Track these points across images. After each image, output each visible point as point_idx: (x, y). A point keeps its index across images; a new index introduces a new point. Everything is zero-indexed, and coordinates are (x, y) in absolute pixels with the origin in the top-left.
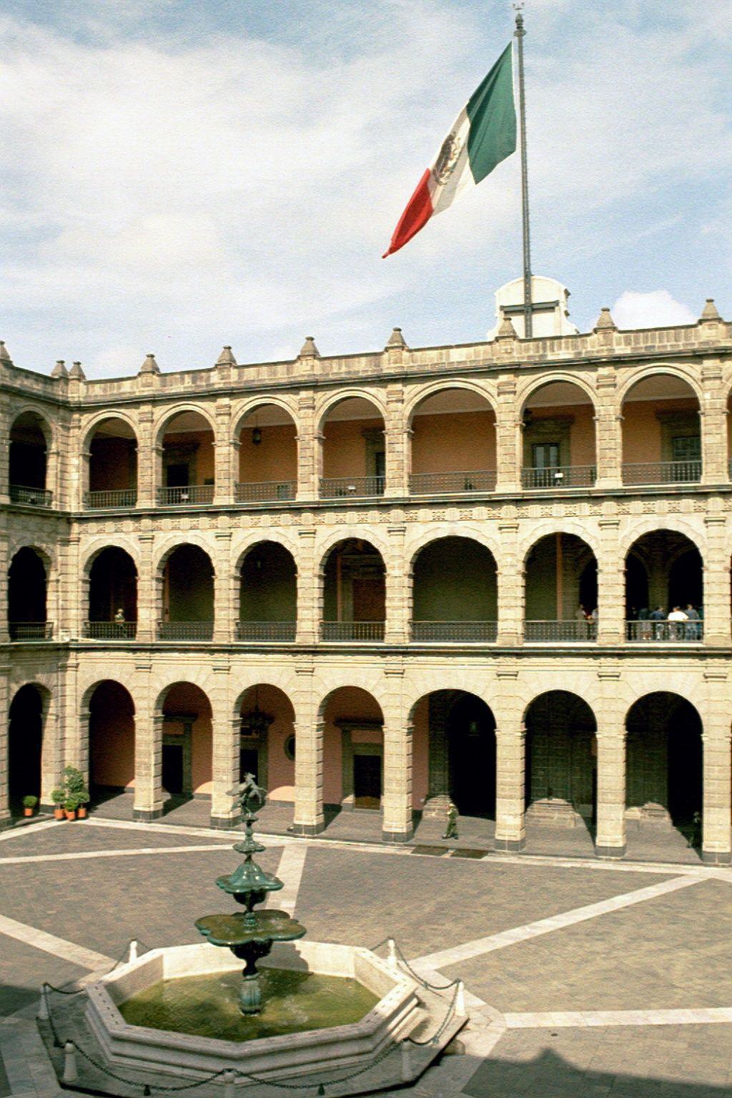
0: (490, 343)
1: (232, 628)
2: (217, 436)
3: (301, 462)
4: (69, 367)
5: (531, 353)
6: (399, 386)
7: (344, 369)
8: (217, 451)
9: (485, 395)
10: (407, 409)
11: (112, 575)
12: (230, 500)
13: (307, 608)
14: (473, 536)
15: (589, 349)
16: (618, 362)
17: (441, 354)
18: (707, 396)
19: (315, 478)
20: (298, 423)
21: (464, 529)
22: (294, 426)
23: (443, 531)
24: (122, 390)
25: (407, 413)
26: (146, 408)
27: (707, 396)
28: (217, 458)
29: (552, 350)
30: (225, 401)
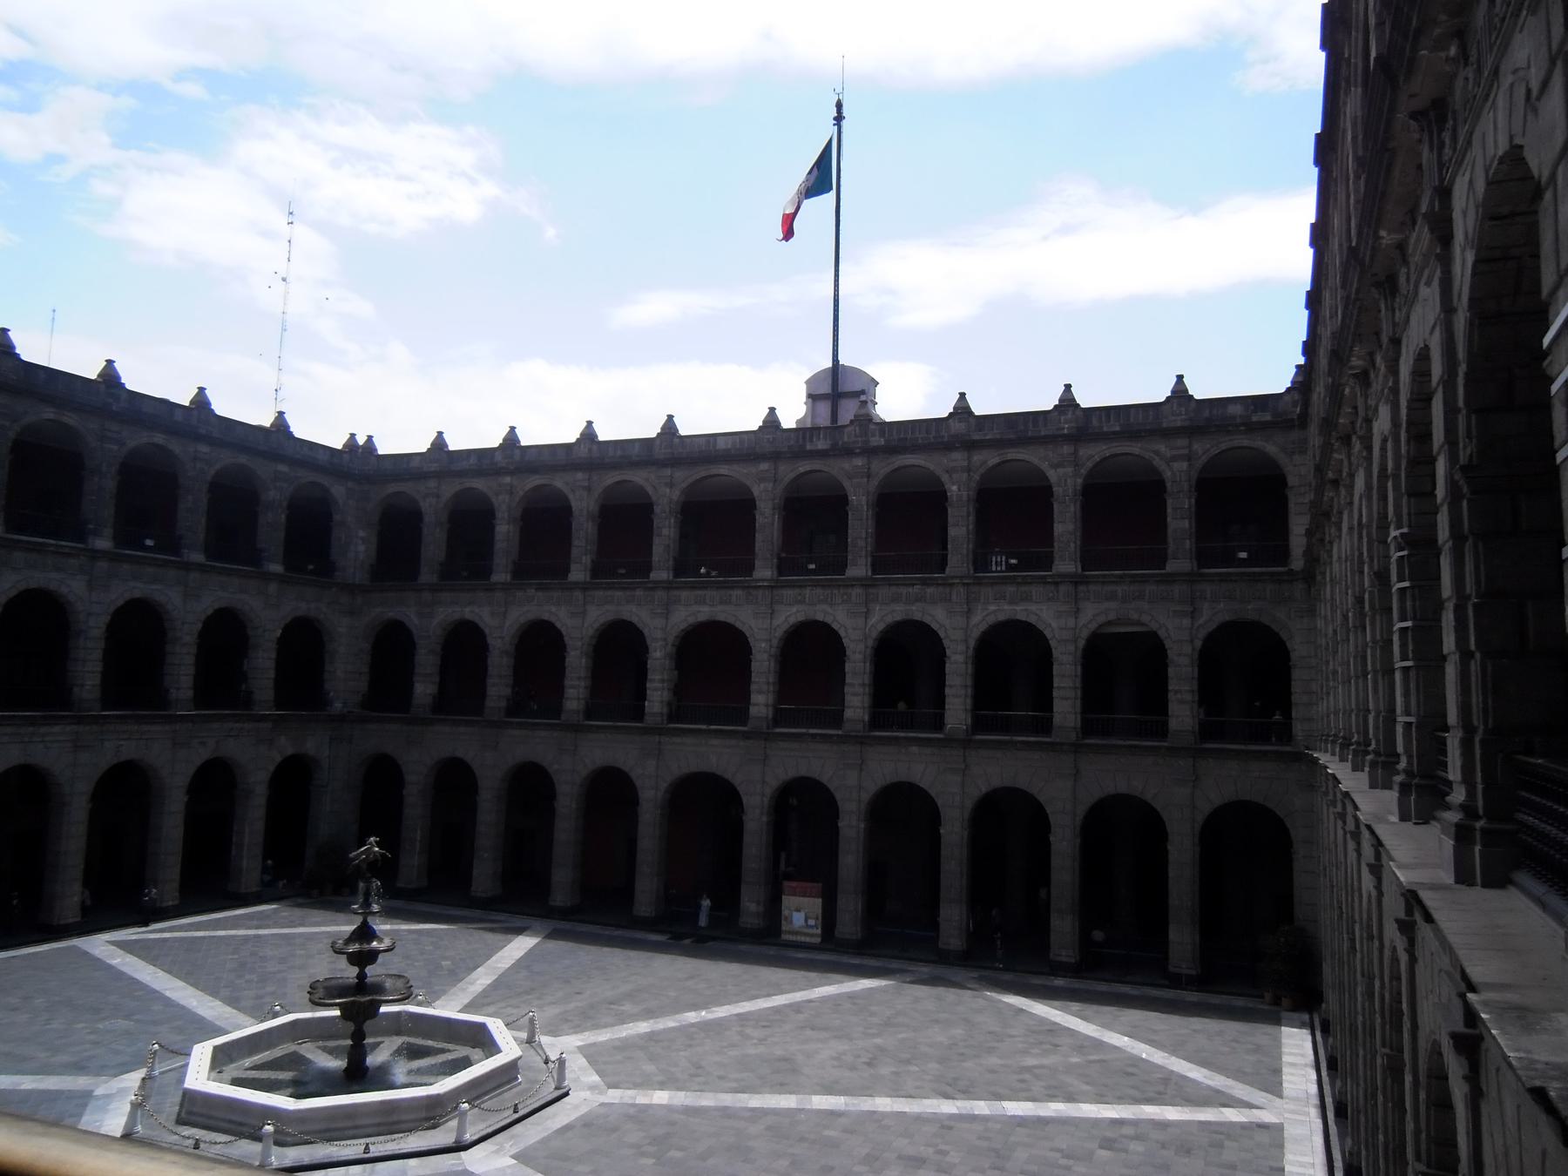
1: (503, 704)
2: (499, 515)
3: (576, 542)
4: (361, 440)
8: (498, 529)
10: (676, 494)
11: (392, 646)
13: (573, 687)
14: (731, 620)
16: (870, 452)
18: (955, 488)
19: (587, 560)
20: (574, 504)
21: (723, 613)
22: (570, 508)
23: (704, 613)
25: (675, 498)
26: (432, 484)
27: (955, 488)
28: (498, 537)
30: (508, 479)
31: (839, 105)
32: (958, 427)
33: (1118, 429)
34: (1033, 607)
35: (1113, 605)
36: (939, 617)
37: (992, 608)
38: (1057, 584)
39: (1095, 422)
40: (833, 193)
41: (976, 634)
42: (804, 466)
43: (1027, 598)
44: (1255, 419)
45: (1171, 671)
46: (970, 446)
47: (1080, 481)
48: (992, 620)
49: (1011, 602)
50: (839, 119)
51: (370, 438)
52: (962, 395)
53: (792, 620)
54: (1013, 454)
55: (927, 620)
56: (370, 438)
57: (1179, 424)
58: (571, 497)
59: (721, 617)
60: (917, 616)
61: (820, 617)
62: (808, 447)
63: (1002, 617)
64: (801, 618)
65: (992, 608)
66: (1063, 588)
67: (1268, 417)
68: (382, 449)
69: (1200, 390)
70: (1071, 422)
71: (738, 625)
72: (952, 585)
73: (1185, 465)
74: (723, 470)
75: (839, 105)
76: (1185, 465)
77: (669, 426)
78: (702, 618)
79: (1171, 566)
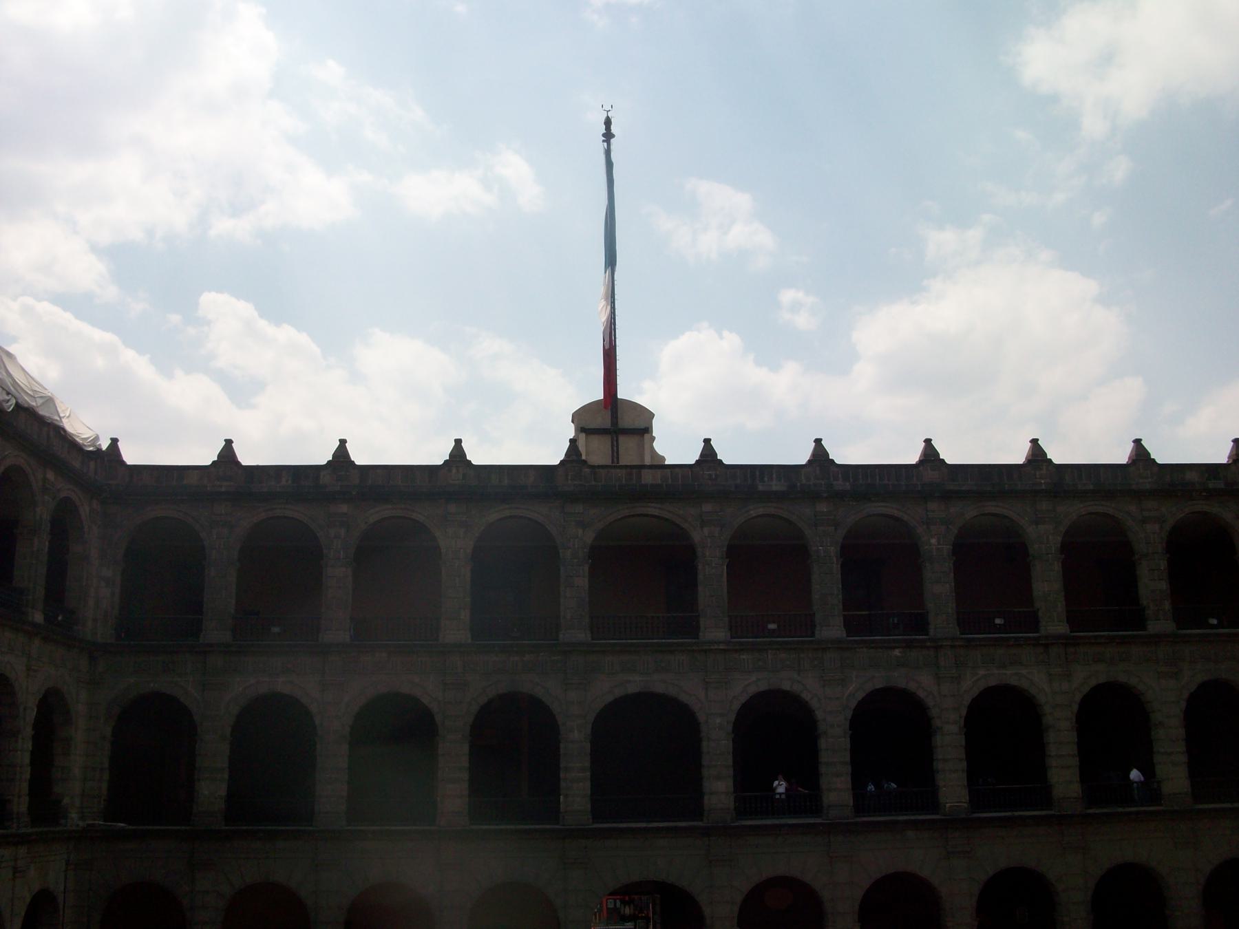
5: (738, 481)
7: (506, 482)
9: (685, 526)
10: (589, 537)
12: (582, 636)
15: (804, 482)
21: (661, 684)
23: (634, 683)
24: (185, 482)
30: (344, 508)
31: (608, 122)
32: (930, 475)
33: (1091, 487)
36: (923, 683)
37: (982, 672)
38: (1046, 646)
41: (967, 700)
42: (756, 510)
44: (1211, 486)
45: (822, 743)
46: (948, 496)
47: (1059, 539)
48: (982, 685)
50: (608, 136)
51: (114, 441)
53: (753, 690)
54: (992, 507)
55: (912, 686)
56: (114, 441)
57: (1148, 487)
59: (659, 688)
60: (901, 683)
61: (786, 686)
62: (760, 488)
63: (993, 682)
64: (763, 686)
65: (982, 672)
67: (1221, 485)
68: (131, 456)
71: (684, 698)
72: (941, 646)
73: (1157, 527)
74: (653, 509)
75: (608, 122)
76: (1157, 527)
78: (632, 689)
79: (1153, 627)
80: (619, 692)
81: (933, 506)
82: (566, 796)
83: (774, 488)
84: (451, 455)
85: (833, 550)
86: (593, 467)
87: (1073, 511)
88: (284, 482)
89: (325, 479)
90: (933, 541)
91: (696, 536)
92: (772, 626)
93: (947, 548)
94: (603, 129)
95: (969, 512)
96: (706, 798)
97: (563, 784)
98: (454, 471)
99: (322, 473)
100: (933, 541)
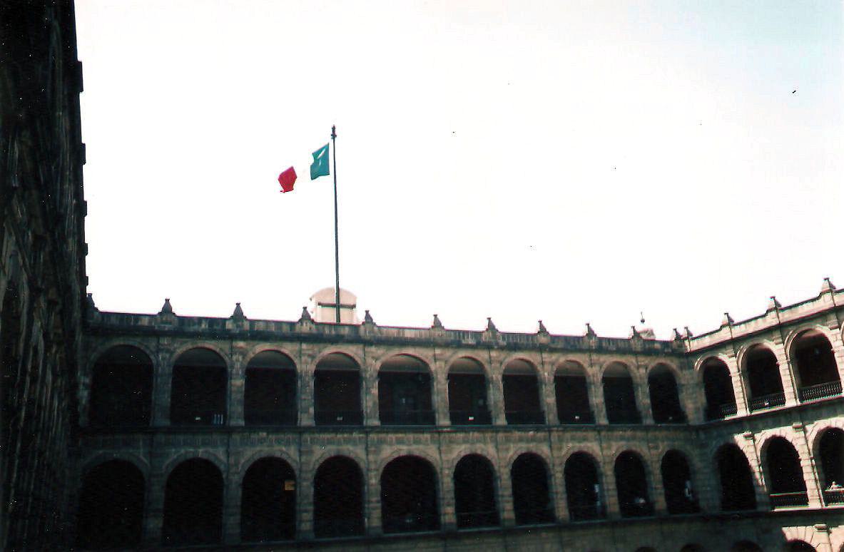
0: (429, 329)
6: (373, 349)
7: (333, 332)
10: (378, 365)
14: (423, 455)
17: (399, 332)
23: (404, 450)
24: (140, 323)
26: (165, 341)
29: (464, 338)
30: (241, 344)
31: (334, 129)
32: (543, 340)
34: (589, 444)
35: (623, 443)
36: (544, 450)
39: (604, 345)
40: (330, 178)
43: (585, 439)
46: (553, 350)
48: (571, 452)
49: (580, 442)
52: (167, 301)
53: (463, 454)
54: (572, 357)
58: (296, 361)
59: (417, 453)
60: (534, 450)
66: (603, 433)
69: (180, 310)
70: (236, 328)
71: (429, 458)
74: (411, 351)
75: (334, 129)
77: (167, 309)
78: (403, 453)
80: (396, 456)
81: (545, 355)
82: (369, 518)
83: (470, 343)
84: (234, 313)
85: (500, 377)
86: (379, 327)
87: (607, 360)
88: (203, 326)
89: (229, 325)
90: (546, 374)
91: (433, 367)
92: (471, 418)
93: (552, 378)
94: (331, 132)
95: (562, 359)
96: (442, 517)
97: (366, 511)
98: (304, 324)
99: (227, 322)
100: (546, 374)
